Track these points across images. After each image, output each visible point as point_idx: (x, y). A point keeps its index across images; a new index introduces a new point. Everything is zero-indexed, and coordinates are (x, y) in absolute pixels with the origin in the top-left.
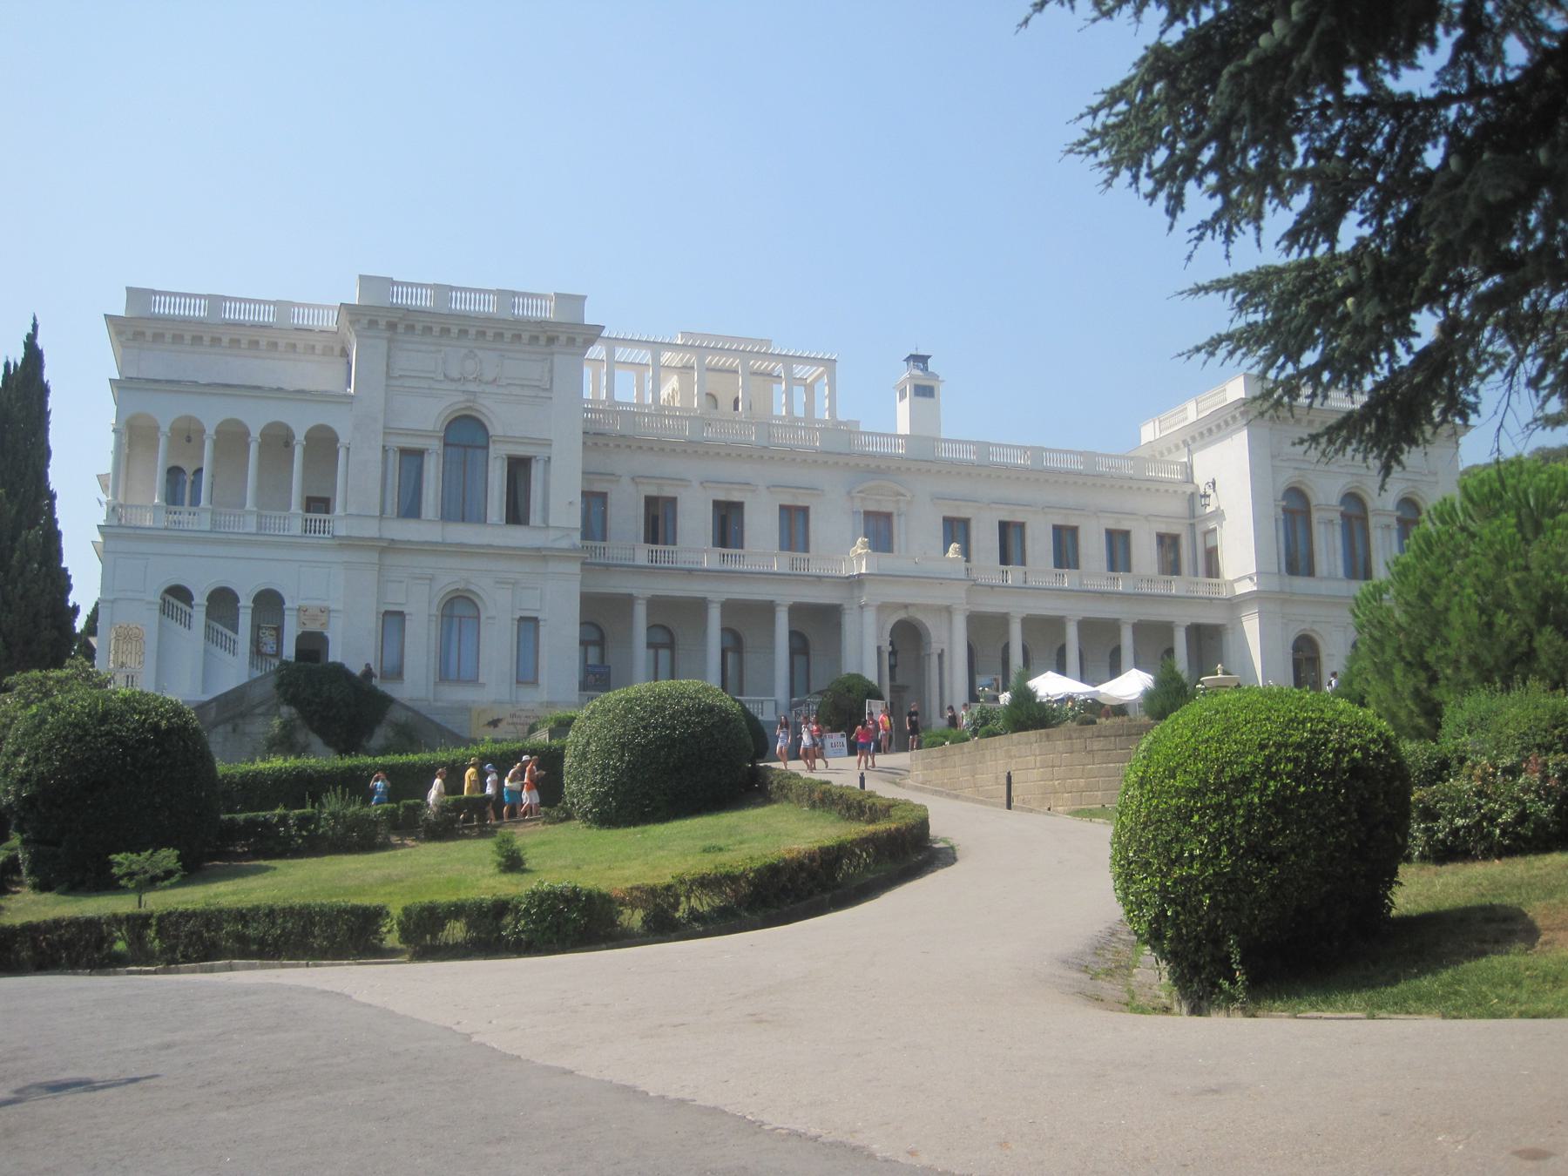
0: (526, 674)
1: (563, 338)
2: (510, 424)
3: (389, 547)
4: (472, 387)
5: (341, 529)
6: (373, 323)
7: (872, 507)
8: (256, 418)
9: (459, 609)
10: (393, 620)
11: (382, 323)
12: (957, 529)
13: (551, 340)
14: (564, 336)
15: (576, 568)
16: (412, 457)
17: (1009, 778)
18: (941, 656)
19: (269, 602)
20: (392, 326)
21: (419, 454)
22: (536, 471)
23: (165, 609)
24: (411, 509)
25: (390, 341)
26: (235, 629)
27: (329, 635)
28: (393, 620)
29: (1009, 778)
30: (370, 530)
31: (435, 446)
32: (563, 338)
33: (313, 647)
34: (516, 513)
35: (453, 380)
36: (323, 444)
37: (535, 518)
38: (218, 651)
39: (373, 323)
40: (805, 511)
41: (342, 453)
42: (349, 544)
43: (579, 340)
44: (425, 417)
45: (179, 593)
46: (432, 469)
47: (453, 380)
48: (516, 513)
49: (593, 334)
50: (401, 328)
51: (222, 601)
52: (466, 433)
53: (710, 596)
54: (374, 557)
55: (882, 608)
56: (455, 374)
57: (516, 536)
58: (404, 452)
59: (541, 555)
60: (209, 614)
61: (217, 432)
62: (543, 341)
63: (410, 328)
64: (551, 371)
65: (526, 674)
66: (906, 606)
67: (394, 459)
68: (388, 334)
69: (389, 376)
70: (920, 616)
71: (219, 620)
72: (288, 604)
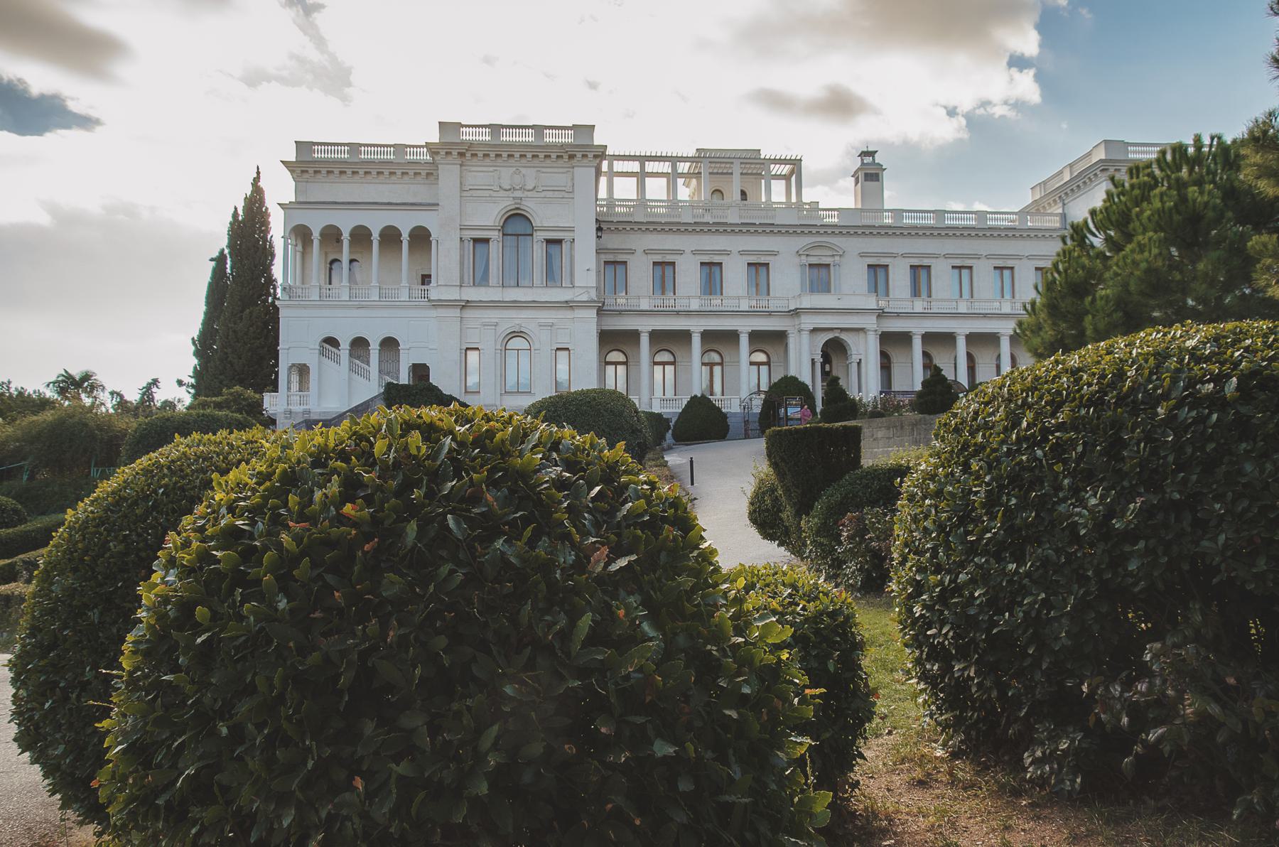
2: (546, 217)
3: (466, 305)
4: (518, 194)
5: (434, 294)
7: (814, 260)
8: (376, 222)
12: (877, 271)
13: (572, 157)
14: (581, 151)
15: (593, 313)
18: (859, 364)
20: (461, 155)
21: (486, 241)
23: (322, 353)
24: (481, 279)
26: (368, 363)
30: (453, 294)
31: (494, 235)
36: (421, 238)
38: (355, 376)
41: (434, 243)
44: (488, 216)
45: (332, 342)
46: (494, 249)
48: (552, 276)
49: (600, 154)
50: (468, 155)
51: (360, 344)
52: (516, 223)
53: (692, 329)
54: (457, 312)
55: (815, 330)
58: (476, 241)
59: (569, 305)
60: (351, 355)
61: (381, 235)
62: (566, 157)
66: (831, 329)
69: (462, 191)
70: (843, 336)
71: (358, 358)
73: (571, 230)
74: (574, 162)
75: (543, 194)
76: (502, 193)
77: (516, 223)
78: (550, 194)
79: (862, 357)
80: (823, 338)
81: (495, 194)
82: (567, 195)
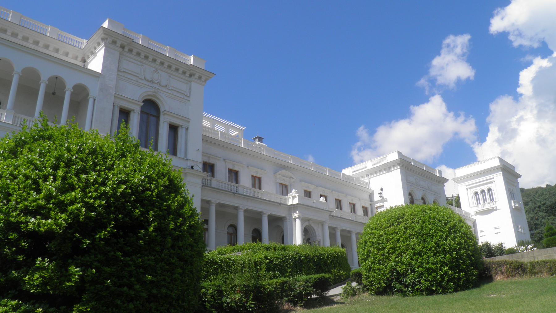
1: (197, 76)
6: (114, 42)
11: (119, 44)
13: (191, 76)
16: (125, 114)
20: (123, 47)
22: (181, 133)
25: (121, 54)
32: (197, 76)
34: (173, 150)
35: (148, 81)
39: (114, 42)
41: (91, 101)
43: (203, 78)
46: (135, 119)
47: (148, 81)
48: (173, 150)
50: (126, 49)
52: (151, 108)
56: (148, 77)
63: (131, 51)
64: (190, 89)
68: (121, 50)
69: (118, 70)
74: (192, 78)
75: (170, 92)
76: (144, 82)
78: (175, 93)
79: (321, 238)
80: (306, 224)
81: (140, 81)
82: (186, 98)
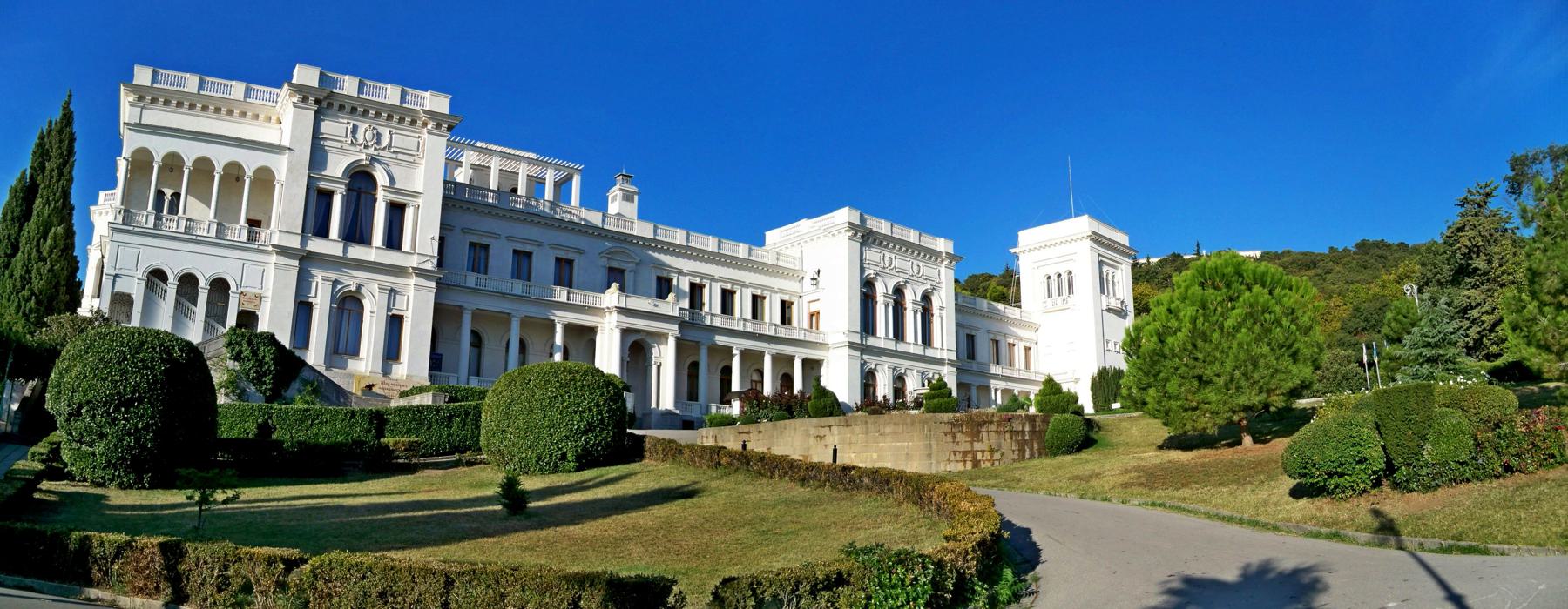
0: (392, 352)
9: (348, 306)
10: (303, 310)
17: (835, 451)
19: (220, 287)
24: (322, 232)
27: (259, 313)
28: (303, 310)
29: (835, 451)
30: (295, 242)
33: (248, 319)
36: (265, 180)
37: (406, 246)
40: (486, 247)
42: (282, 251)
45: (158, 275)
48: (393, 240)
51: (188, 283)
57: (392, 258)
65: (392, 352)
67: (314, 196)
72: (233, 288)
73: (414, 194)
77: (361, 180)
